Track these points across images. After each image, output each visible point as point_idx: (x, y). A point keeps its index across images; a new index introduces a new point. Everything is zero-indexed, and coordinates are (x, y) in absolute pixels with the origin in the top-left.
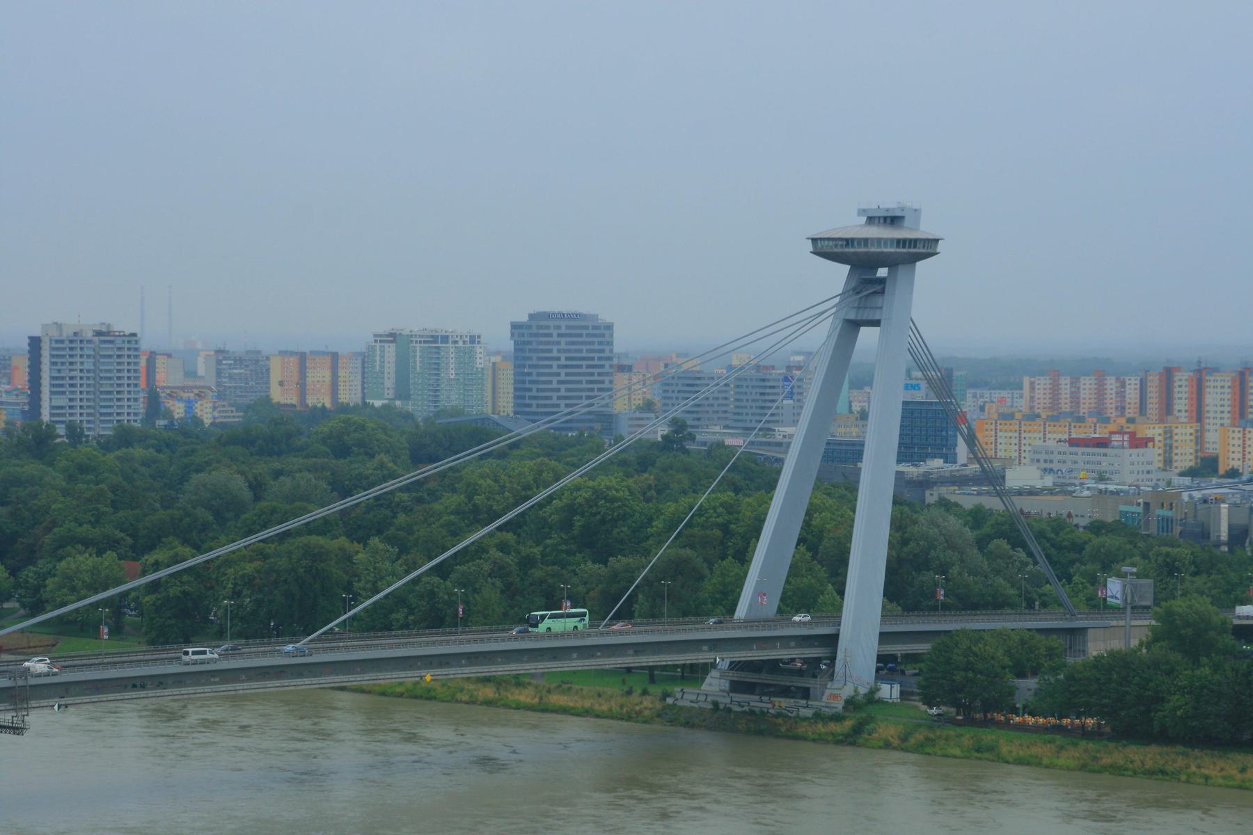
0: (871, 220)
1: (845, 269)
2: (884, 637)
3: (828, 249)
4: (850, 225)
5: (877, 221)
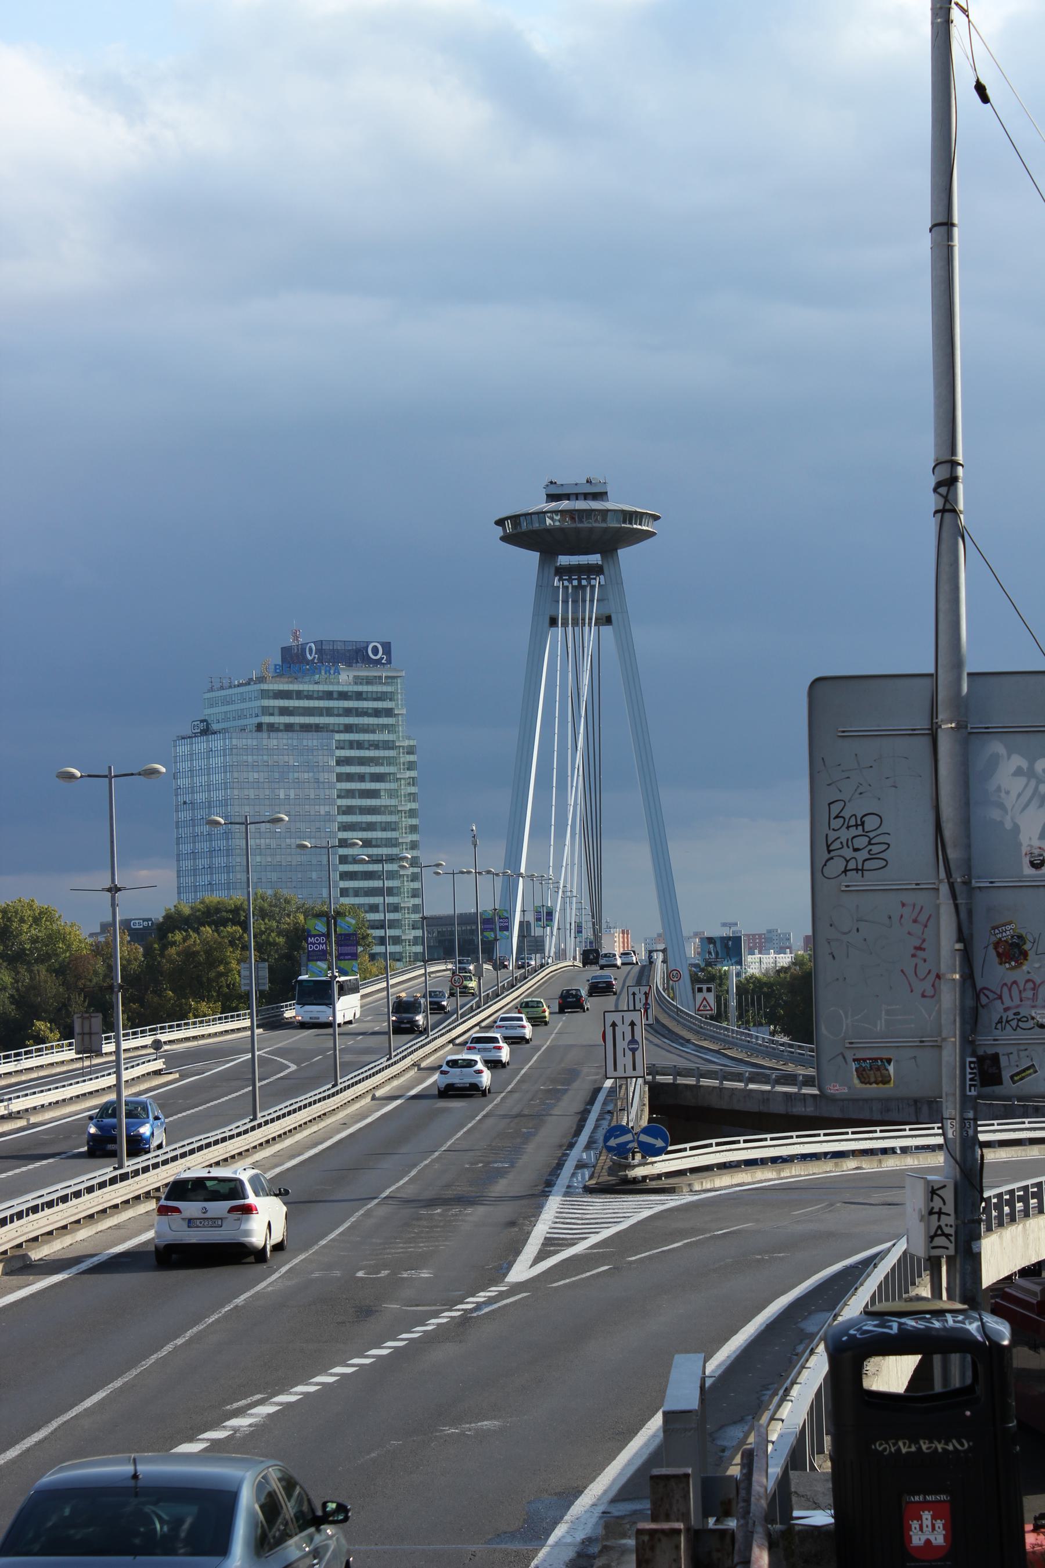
0: (552, 497)
1: (539, 553)
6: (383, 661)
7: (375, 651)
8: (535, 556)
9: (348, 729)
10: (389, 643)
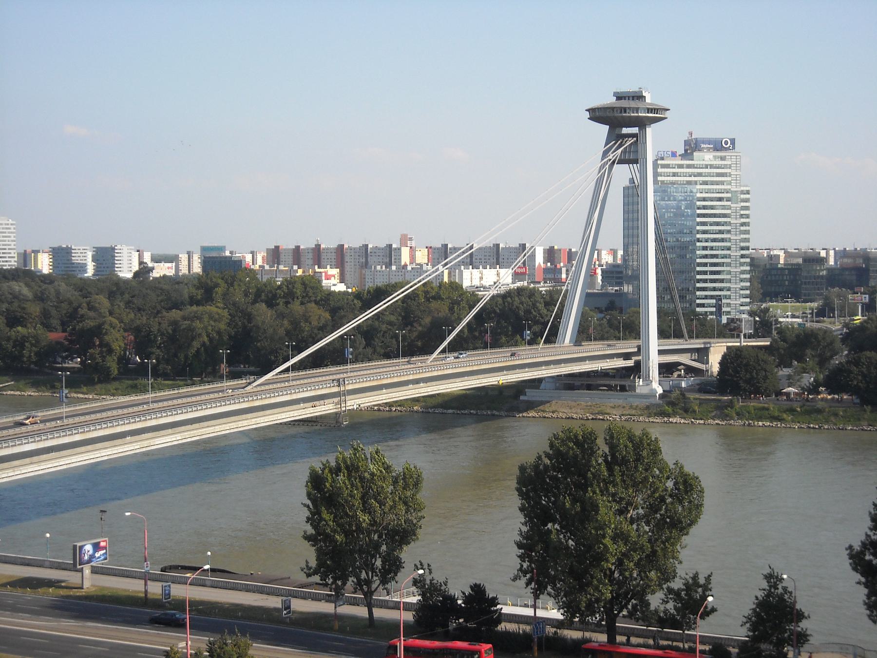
2: (661, 352)
3: (598, 115)
4: (609, 100)
5: (627, 98)
6: (731, 148)
7: (726, 143)
8: (606, 128)
9: (705, 183)
10: (734, 139)
